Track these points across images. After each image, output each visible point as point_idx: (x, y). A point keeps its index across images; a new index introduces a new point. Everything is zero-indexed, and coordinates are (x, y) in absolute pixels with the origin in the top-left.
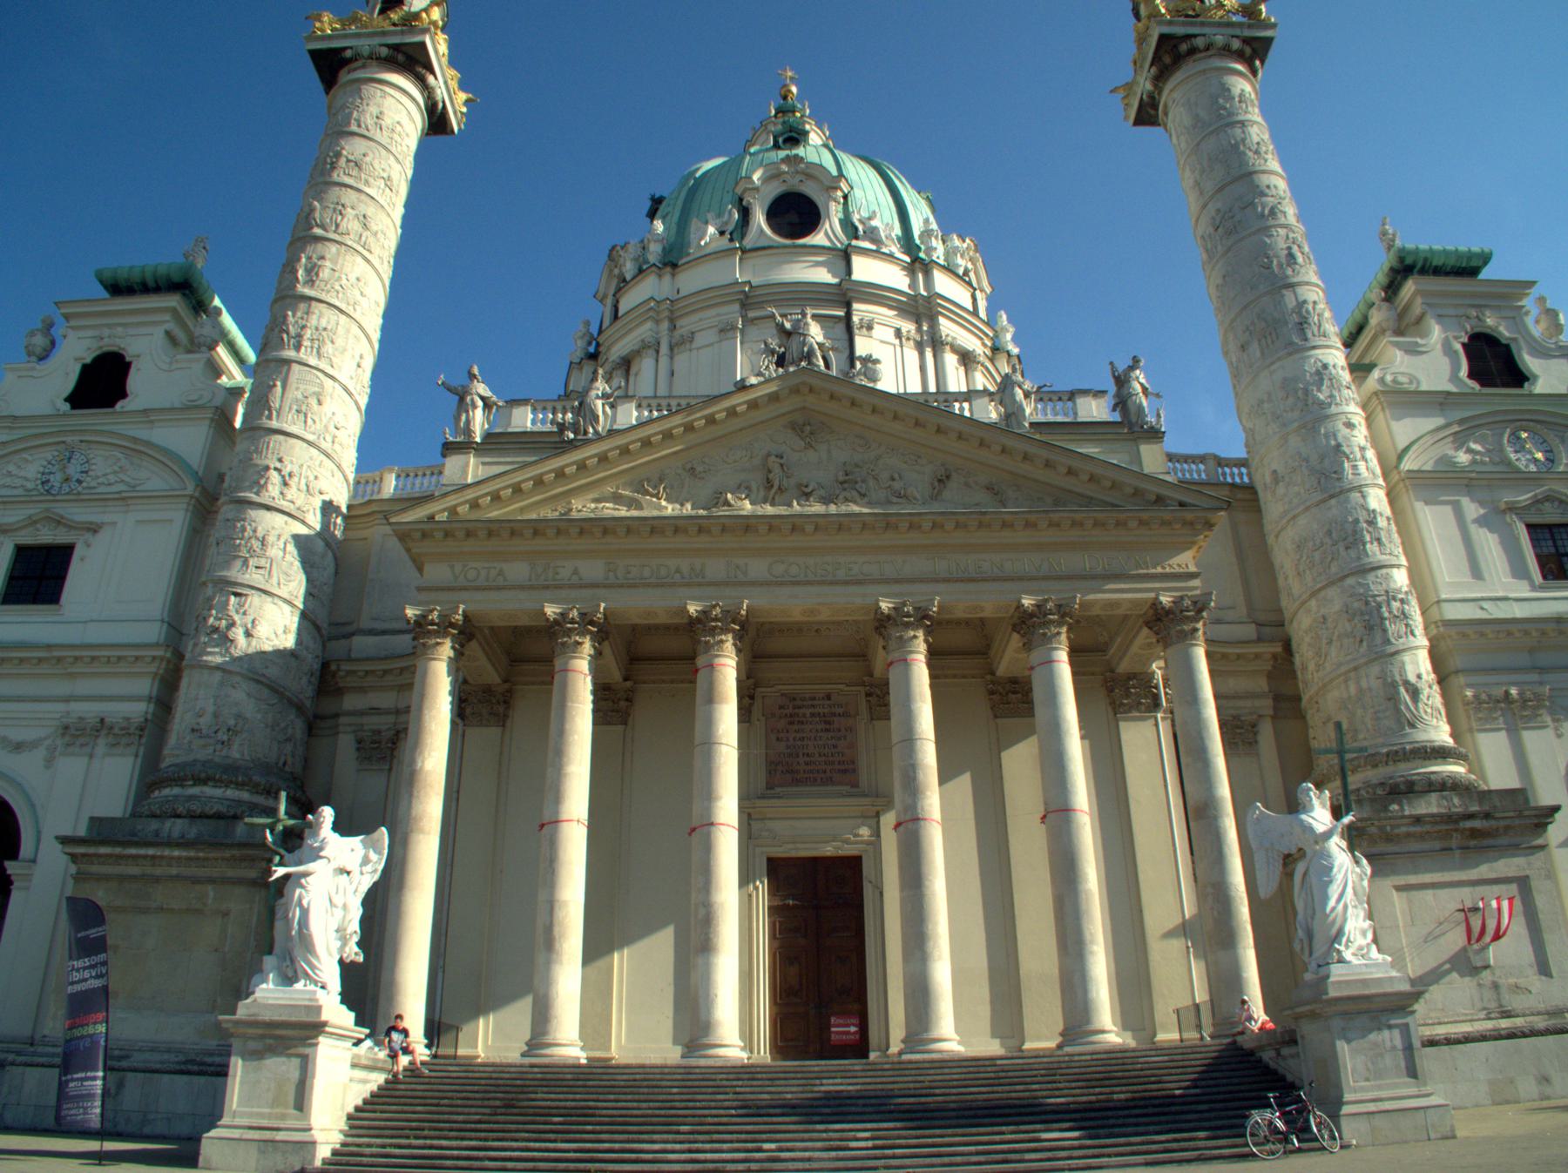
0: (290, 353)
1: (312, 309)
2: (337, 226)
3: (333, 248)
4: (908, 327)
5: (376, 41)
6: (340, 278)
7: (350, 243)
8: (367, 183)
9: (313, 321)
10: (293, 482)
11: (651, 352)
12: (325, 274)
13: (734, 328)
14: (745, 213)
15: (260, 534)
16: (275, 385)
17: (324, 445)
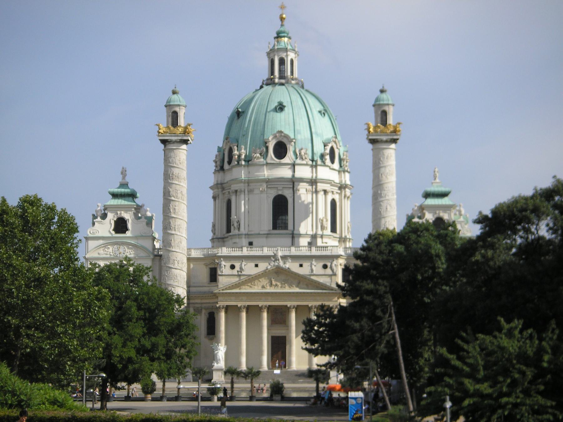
0: (173, 232)
1: (176, 220)
2: (177, 197)
3: (177, 203)
4: (310, 188)
5: (176, 138)
6: (179, 211)
7: (180, 201)
8: (181, 182)
9: (176, 224)
10: (179, 263)
11: (243, 193)
12: (177, 211)
13: (264, 190)
14: (267, 148)
15: (175, 274)
16: (171, 240)
17: (183, 253)
